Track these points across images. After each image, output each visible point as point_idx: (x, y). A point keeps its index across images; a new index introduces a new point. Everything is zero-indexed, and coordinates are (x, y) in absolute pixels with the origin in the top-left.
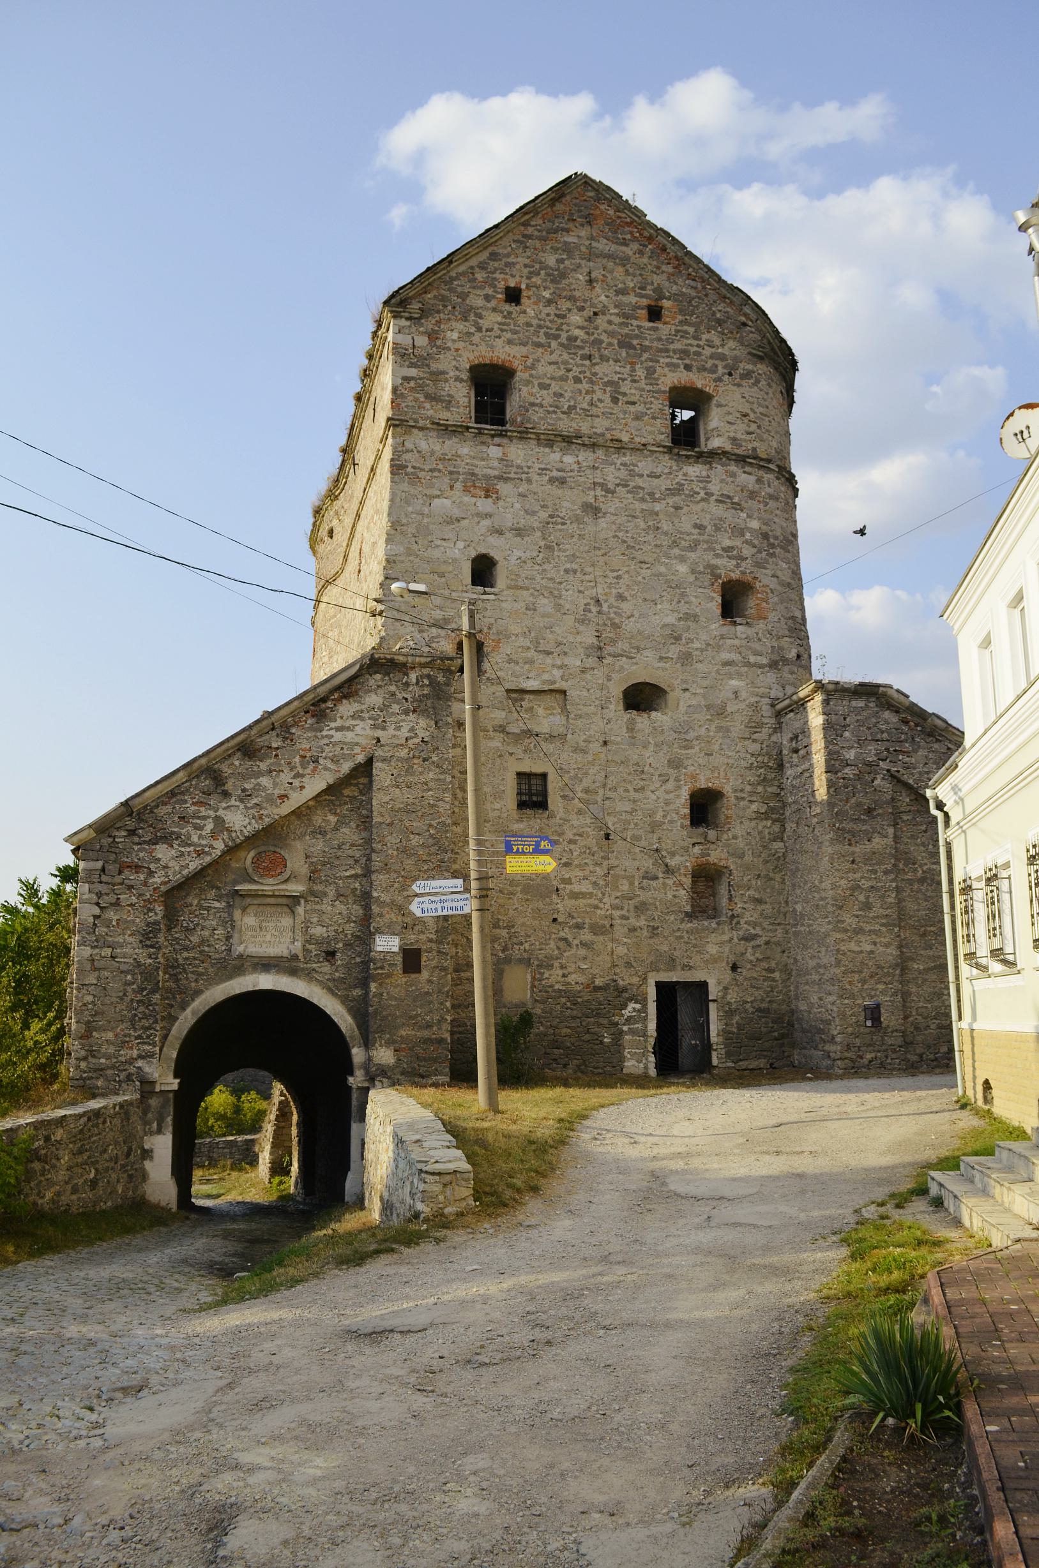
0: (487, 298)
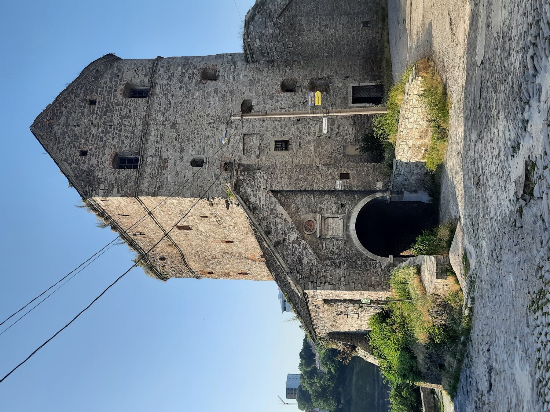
0: (84, 163)
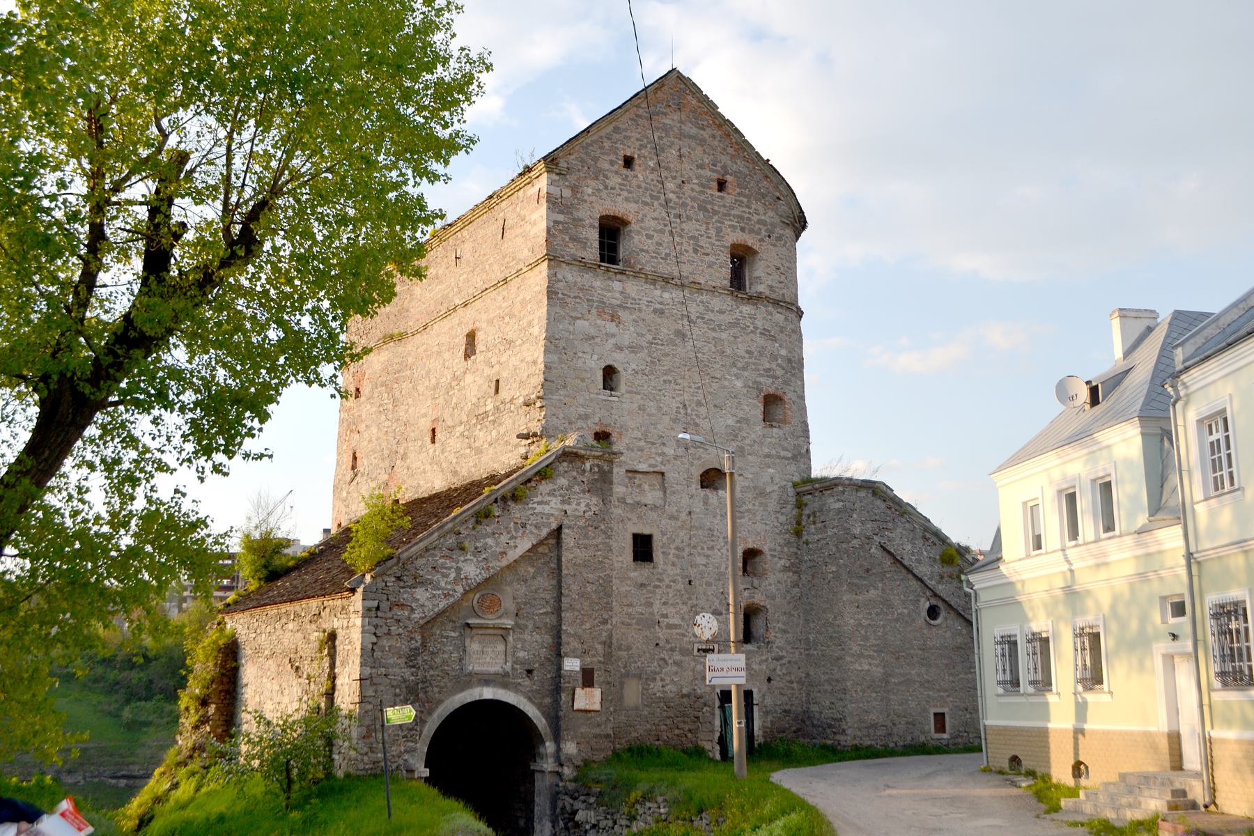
0: (612, 163)
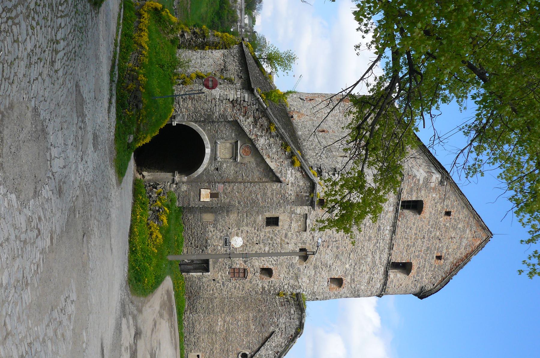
0: (447, 206)
